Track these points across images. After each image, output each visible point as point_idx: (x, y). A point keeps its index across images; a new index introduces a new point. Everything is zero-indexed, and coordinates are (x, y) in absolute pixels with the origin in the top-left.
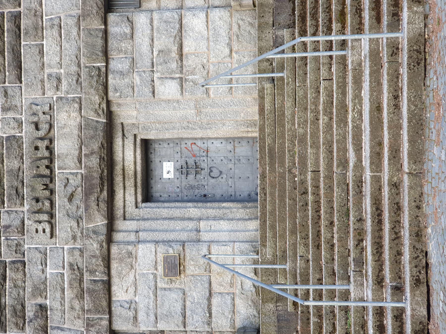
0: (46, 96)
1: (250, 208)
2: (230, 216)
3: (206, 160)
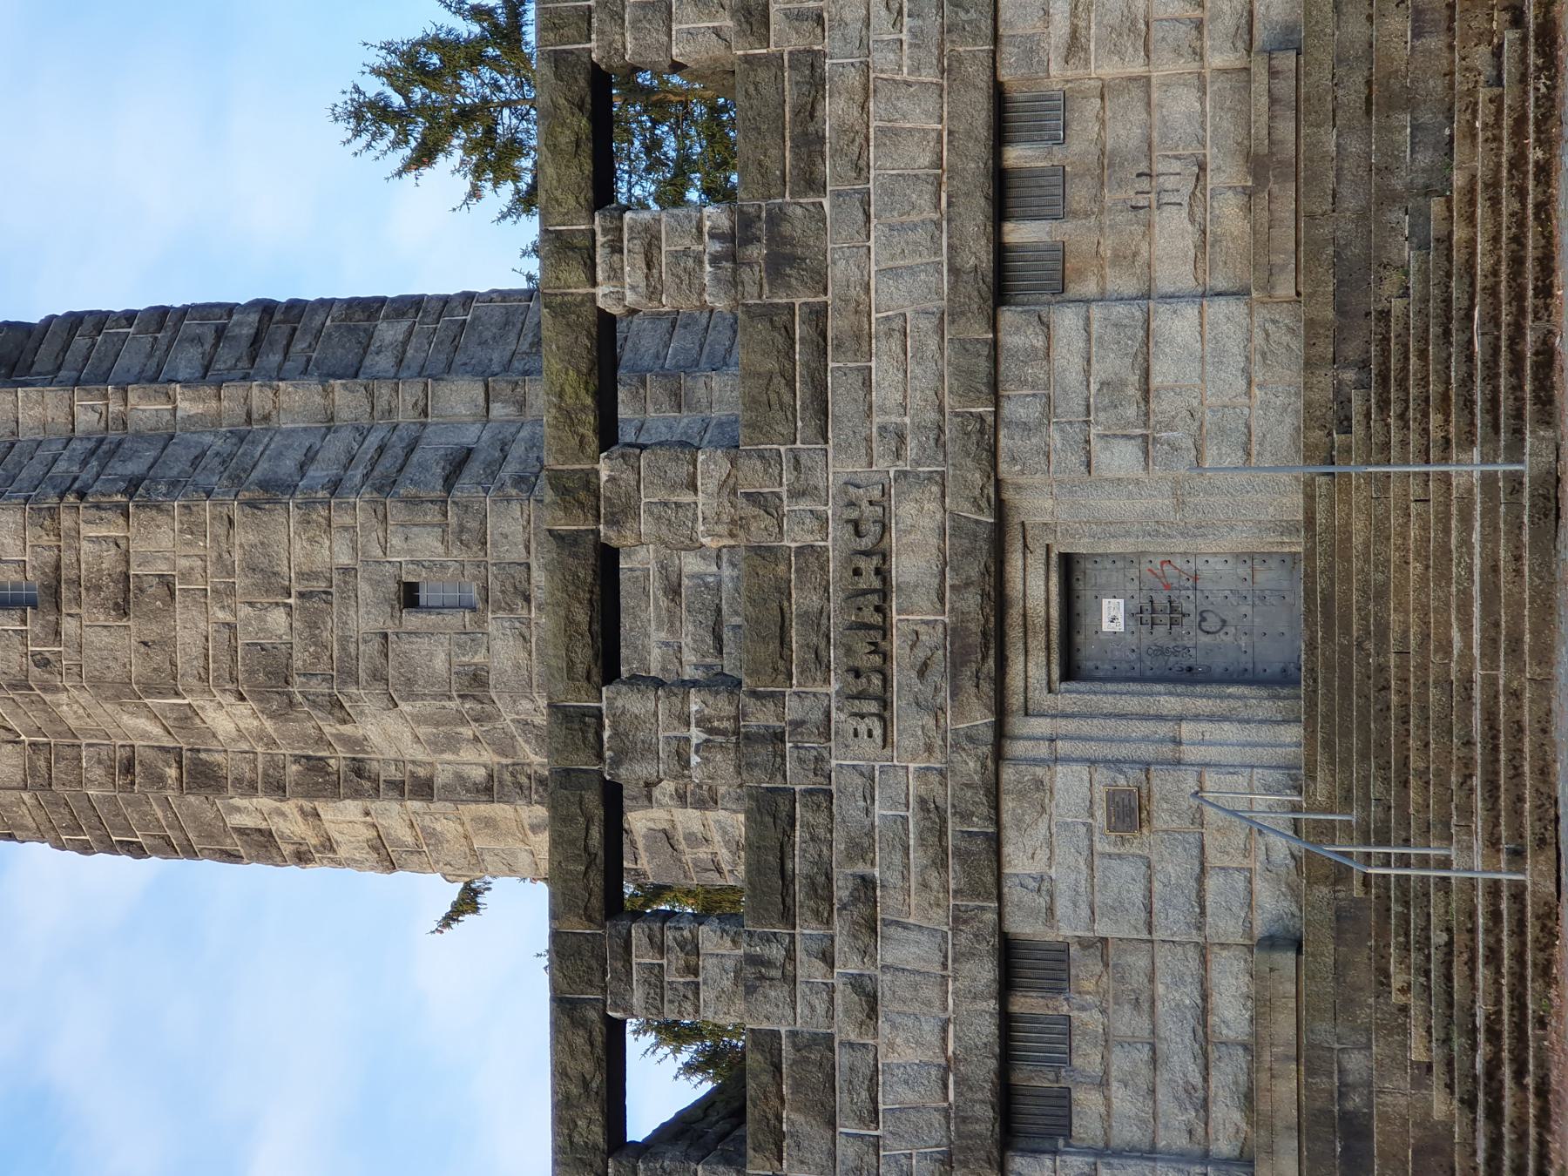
0: (874, 468)
1: (1285, 698)
2: (1244, 714)
3: (1192, 597)
